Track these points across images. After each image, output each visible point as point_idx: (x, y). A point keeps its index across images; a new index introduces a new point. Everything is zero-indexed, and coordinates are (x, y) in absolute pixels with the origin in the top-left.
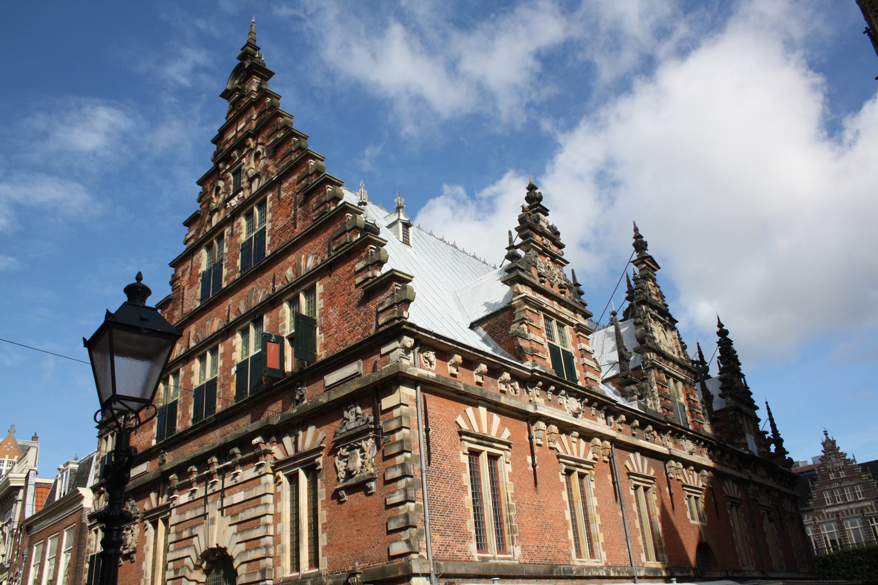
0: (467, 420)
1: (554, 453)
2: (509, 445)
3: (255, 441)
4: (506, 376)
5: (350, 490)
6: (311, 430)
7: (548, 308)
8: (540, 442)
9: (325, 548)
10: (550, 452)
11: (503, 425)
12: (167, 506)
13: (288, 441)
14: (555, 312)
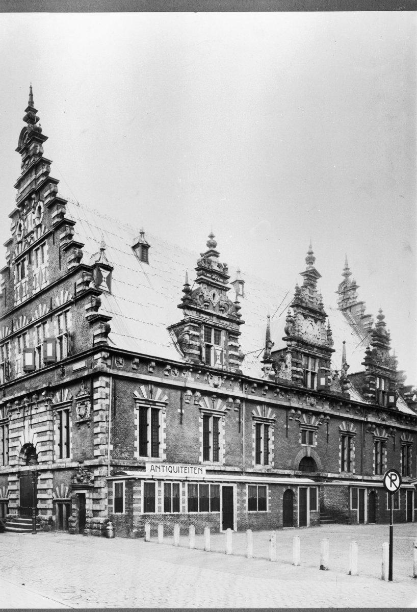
0: (141, 393)
1: (198, 407)
2: (166, 404)
3: (43, 393)
4: (169, 367)
5: (81, 424)
6: (67, 390)
7: (208, 322)
8: (188, 401)
9: (72, 449)
10: (195, 406)
11: (163, 394)
12: (8, 419)
13: (58, 395)
14: (213, 324)
